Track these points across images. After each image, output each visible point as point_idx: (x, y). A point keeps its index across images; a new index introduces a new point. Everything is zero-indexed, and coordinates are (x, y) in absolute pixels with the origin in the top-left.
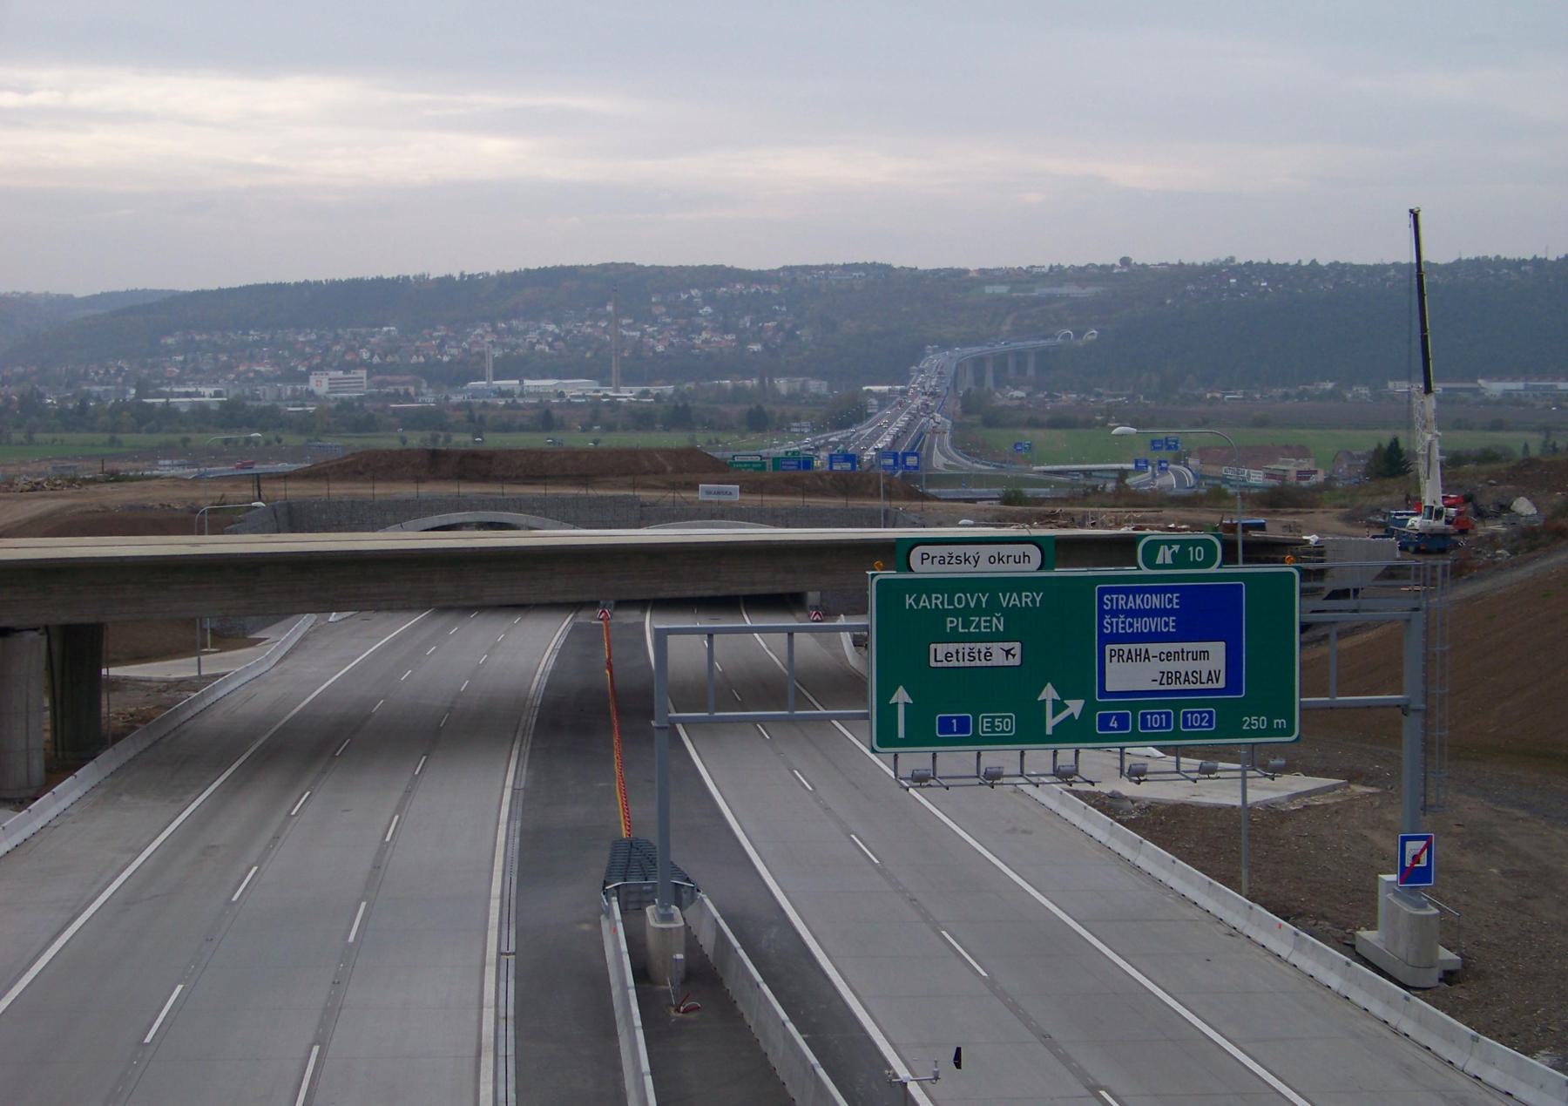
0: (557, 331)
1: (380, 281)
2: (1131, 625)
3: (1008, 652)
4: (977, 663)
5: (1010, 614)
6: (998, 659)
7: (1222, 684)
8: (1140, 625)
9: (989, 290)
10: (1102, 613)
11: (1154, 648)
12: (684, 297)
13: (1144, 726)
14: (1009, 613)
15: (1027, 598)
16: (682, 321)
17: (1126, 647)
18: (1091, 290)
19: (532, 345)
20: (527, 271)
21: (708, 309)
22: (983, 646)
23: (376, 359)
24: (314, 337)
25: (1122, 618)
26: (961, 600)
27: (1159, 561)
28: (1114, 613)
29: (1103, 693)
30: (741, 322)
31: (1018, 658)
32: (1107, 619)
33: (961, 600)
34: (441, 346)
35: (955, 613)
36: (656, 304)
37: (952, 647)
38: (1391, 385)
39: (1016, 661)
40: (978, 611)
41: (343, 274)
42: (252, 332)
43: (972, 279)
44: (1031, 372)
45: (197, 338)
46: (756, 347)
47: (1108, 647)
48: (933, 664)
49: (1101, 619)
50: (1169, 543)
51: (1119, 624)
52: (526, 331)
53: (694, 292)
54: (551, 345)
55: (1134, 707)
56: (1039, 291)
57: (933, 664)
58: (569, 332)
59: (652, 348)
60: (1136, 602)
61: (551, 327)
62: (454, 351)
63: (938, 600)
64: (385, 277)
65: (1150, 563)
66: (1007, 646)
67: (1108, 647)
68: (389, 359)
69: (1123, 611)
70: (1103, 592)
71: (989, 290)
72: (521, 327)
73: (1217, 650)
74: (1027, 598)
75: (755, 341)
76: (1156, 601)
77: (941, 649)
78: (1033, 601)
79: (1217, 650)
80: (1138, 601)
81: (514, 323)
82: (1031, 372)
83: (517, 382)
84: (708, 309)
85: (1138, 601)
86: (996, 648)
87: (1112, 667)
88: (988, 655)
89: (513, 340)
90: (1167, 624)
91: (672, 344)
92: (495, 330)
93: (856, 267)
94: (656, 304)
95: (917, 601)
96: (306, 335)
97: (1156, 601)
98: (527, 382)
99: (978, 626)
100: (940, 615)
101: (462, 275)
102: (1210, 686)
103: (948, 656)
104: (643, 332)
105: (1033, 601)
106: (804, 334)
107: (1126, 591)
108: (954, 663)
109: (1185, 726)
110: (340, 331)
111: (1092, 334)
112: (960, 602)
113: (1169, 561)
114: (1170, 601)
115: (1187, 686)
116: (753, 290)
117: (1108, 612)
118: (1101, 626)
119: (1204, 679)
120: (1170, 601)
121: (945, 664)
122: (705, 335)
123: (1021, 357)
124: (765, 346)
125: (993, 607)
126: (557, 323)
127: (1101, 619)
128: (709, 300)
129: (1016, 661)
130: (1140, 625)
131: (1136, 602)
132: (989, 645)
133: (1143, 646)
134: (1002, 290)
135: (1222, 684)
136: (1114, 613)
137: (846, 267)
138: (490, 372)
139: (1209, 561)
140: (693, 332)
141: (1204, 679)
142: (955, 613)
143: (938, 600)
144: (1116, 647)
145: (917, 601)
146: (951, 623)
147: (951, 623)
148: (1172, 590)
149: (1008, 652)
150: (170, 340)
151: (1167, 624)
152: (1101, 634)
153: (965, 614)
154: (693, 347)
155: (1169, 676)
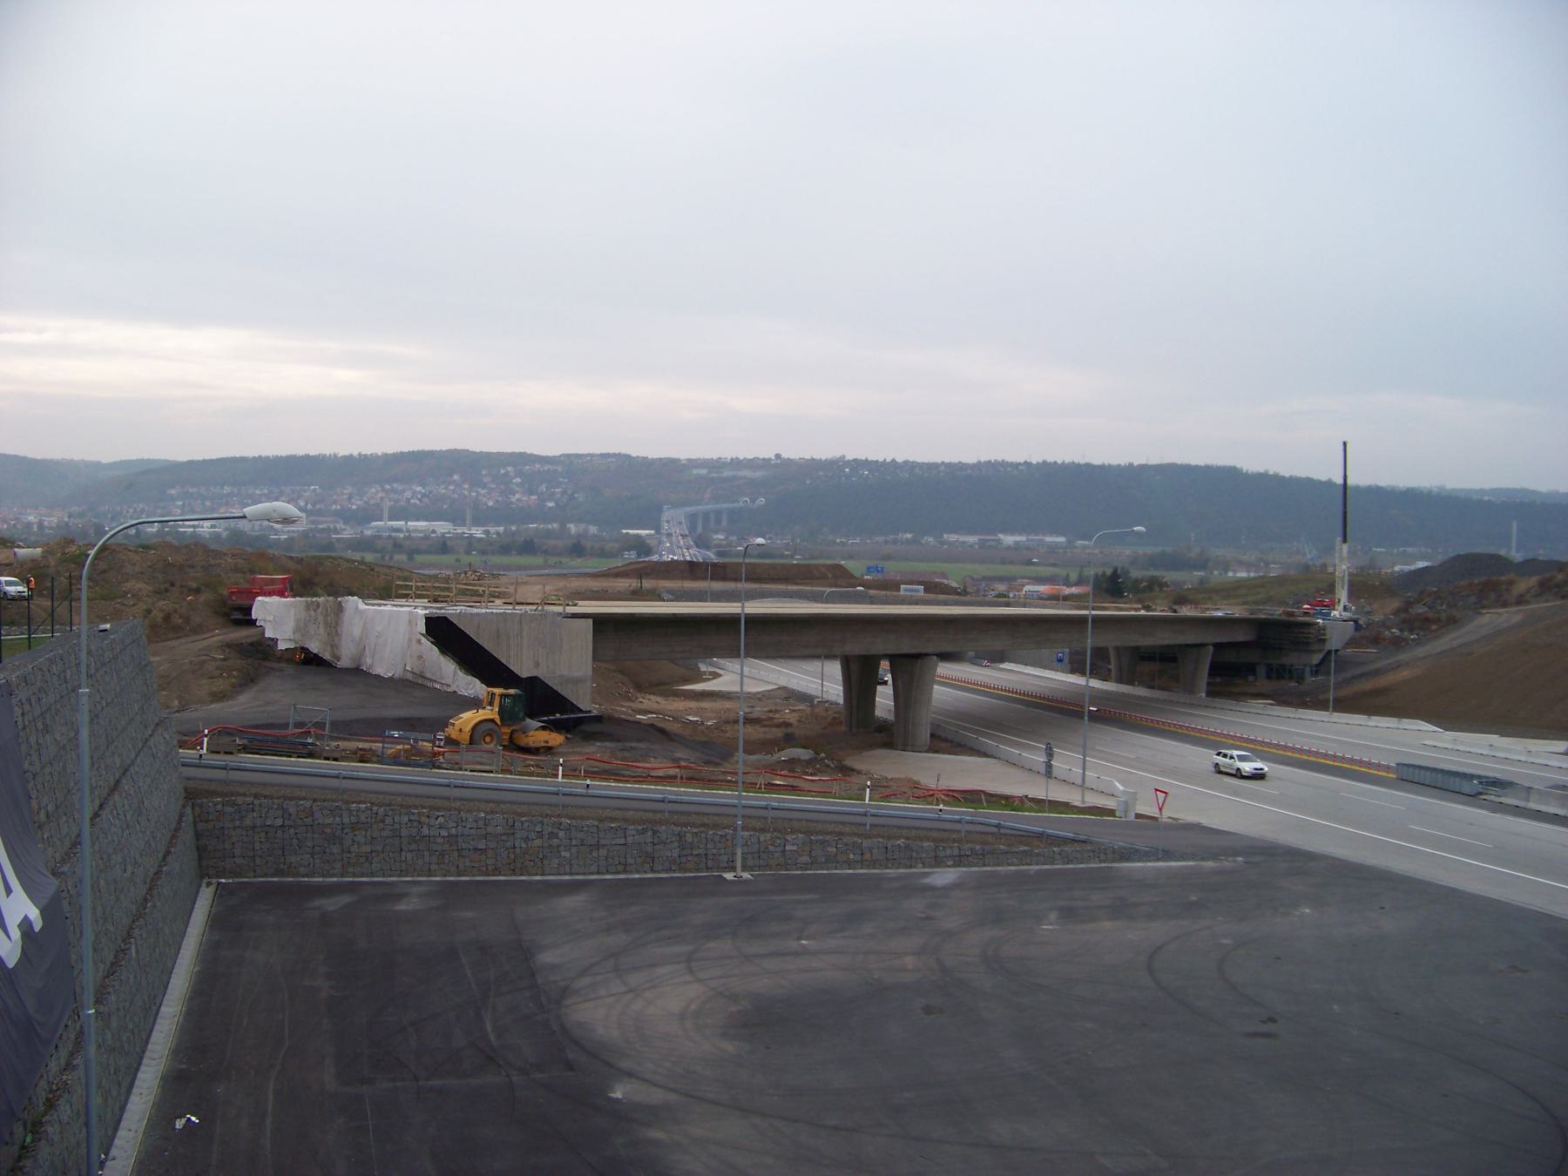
0: (423, 491)
1: (307, 456)
9: (695, 471)
12: (503, 471)
16: (502, 487)
18: (759, 474)
19: (408, 500)
20: (402, 453)
21: (518, 480)
23: (309, 506)
24: (266, 491)
30: (540, 488)
34: (350, 498)
36: (485, 476)
38: (945, 536)
41: (283, 451)
42: (226, 488)
43: (684, 465)
44: (724, 523)
45: (191, 490)
46: (550, 504)
52: (404, 491)
53: (509, 469)
54: (420, 500)
56: (727, 474)
58: (431, 492)
59: (486, 504)
61: (419, 489)
62: (359, 503)
64: (311, 454)
68: (318, 507)
71: (695, 471)
72: (400, 488)
75: (550, 500)
81: (395, 485)
82: (724, 523)
83: (403, 523)
84: (518, 480)
89: (396, 497)
91: (497, 501)
92: (384, 490)
93: (608, 455)
94: (485, 476)
96: (261, 490)
98: (409, 523)
101: (359, 454)
104: (478, 492)
106: (580, 497)
110: (283, 488)
111: (762, 501)
116: (546, 468)
122: (517, 496)
123: (718, 513)
124: (557, 504)
126: (423, 486)
128: (520, 473)
134: (703, 472)
137: (602, 455)
138: (386, 515)
140: (510, 494)
150: (173, 492)
154: (511, 502)
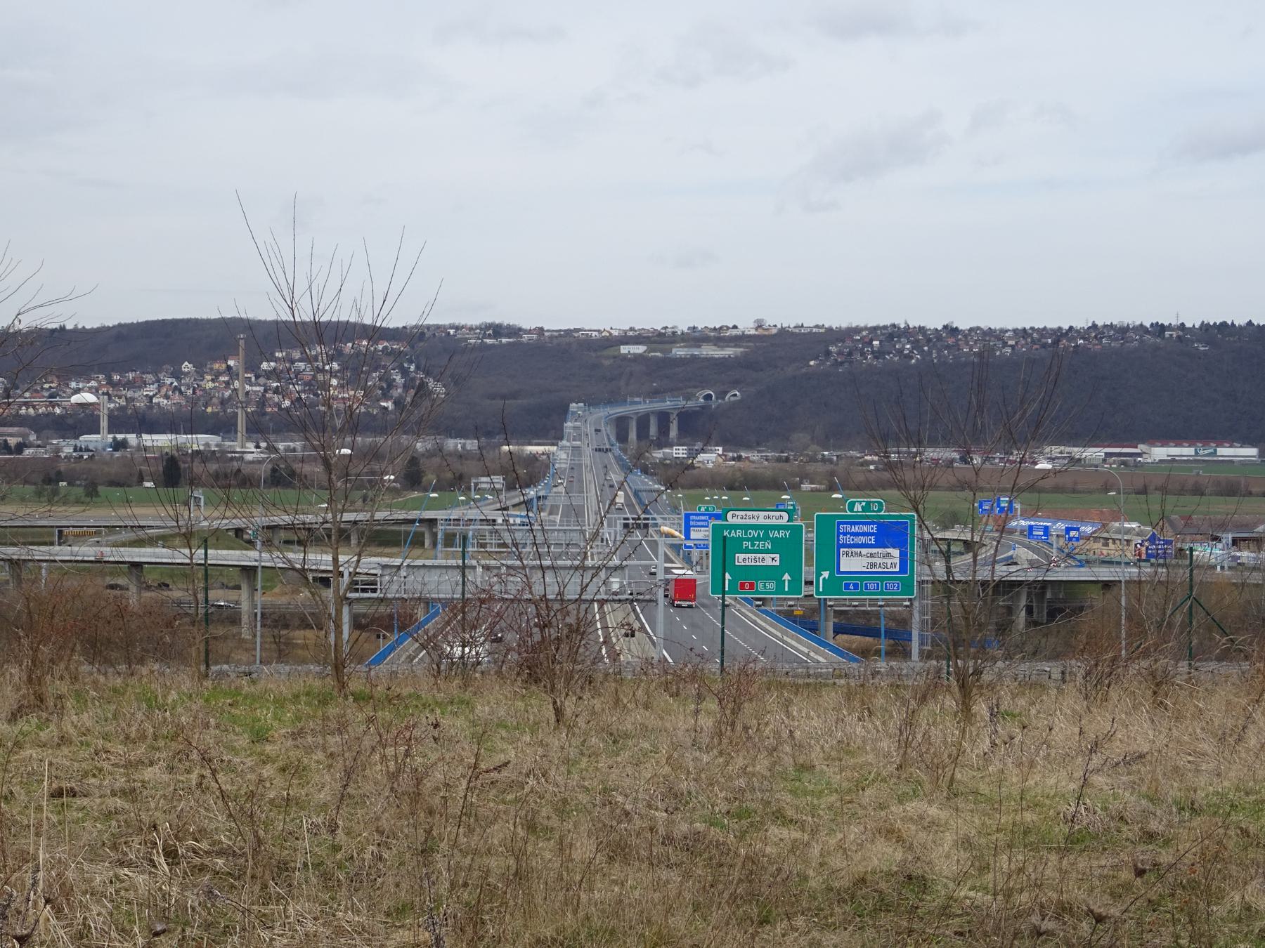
2: (853, 540)
3: (773, 559)
4: (758, 564)
5: (775, 541)
6: (769, 562)
7: (897, 569)
8: (857, 540)
10: (839, 533)
11: (864, 551)
13: (866, 589)
14: (774, 541)
15: (782, 533)
17: (850, 550)
22: (761, 556)
25: (848, 536)
26: (754, 533)
27: (855, 510)
28: (845, 534)
29: (839, 572)
31: (778, 561)
32: (841, 537)
33: (754, 533)
35: (748, 539)
37: (746, 556)
39: (777, 563)
40: (759, 539)
47: (842, 550)
48: (737, 564)
49: (838, 537)
50: (861, 502)
51: (847, 539)
55: (862, 580)
57: (737, 564)
60: (855, 529)
63: (740, 533)
65: (852, 510)
66: (773, 556)
67: (842, 550)
69: (849, 533)
70: (839, 524)
73: (896, 552)
74: (782, 533)
76: (865, 529)
77: (741, 556)
78: (785, 535)
79: (896, 552)
80: (857, 528)
85: (857, 528)
86: (768, 557)
87: (843, 560)
88: (763, 560)
90: (870, 540)
95: (730, 533)
97: (865, 529)
99: (758, 546)
100: (740, 540)
102: (891, 570)
103: (744, 560)
105: (785, 535)
107: (851, 524)
108: (747, 564)
109: (886, 589)
112: (750, 533)
113: (860, 510)
114: (872, 529)
115: (880, 570)
117: (841, 533)
118: (838, 540)
119: (889, 566)
120: (872, 529)
121: (743, 564)
125: (766, 537)
127: (838, 537)
129: (777, 563)
130: (857, 540)
131: (855, 529)
132: (763, 555)
133: (859, 550)
135: (897, 569)
136: (845, 534)
139: (880, 511)
141: (889, 566)
142: (748, 539)
143: (740, 533)
144: (845, 550)
145: (730, 533)
146: (745, 544)
147: (745, 544)
148: (873, 523)
149: (773, 559)
151: (870, 540)
152: (838, 543)
153: (752, 540)
155: (873, 565)
